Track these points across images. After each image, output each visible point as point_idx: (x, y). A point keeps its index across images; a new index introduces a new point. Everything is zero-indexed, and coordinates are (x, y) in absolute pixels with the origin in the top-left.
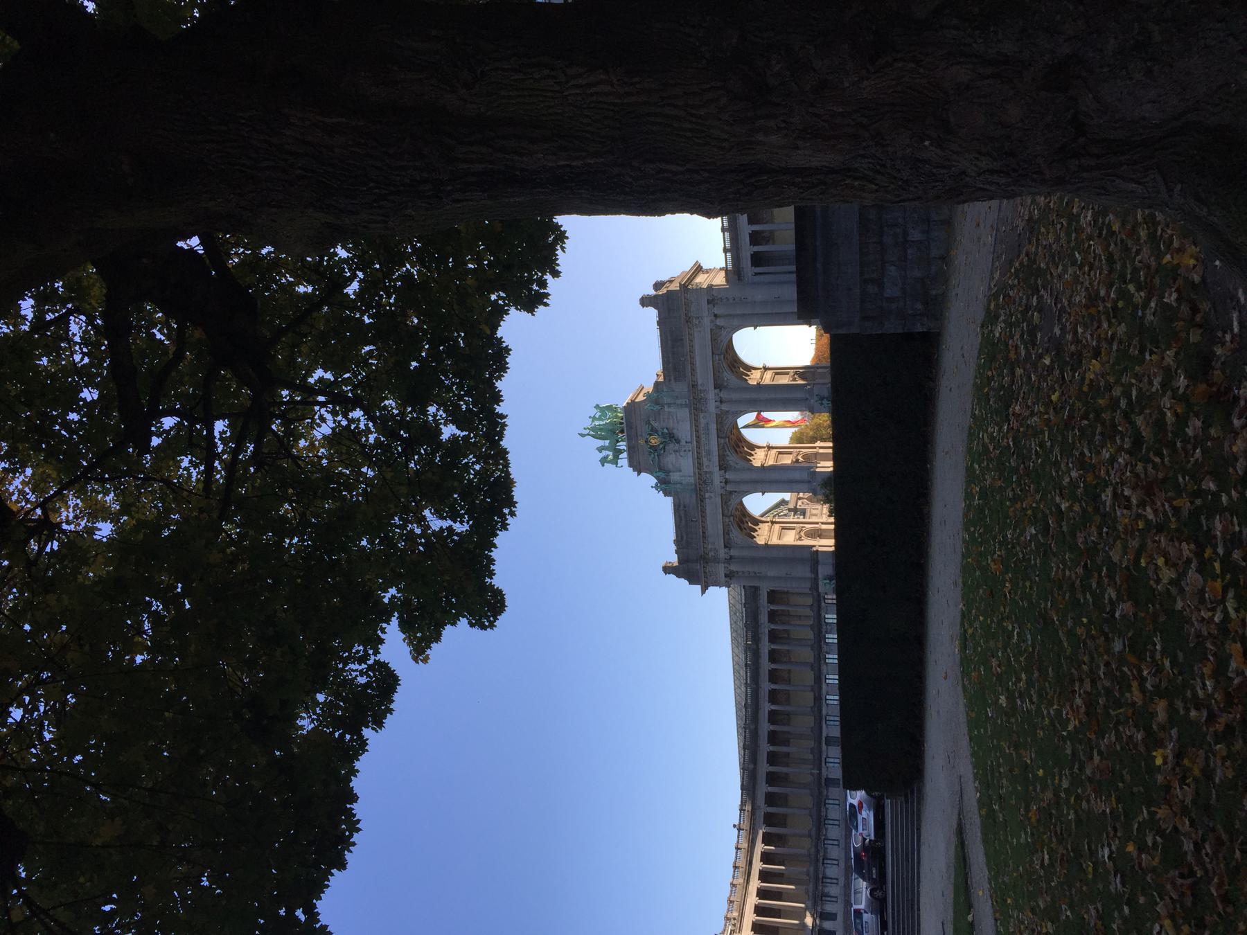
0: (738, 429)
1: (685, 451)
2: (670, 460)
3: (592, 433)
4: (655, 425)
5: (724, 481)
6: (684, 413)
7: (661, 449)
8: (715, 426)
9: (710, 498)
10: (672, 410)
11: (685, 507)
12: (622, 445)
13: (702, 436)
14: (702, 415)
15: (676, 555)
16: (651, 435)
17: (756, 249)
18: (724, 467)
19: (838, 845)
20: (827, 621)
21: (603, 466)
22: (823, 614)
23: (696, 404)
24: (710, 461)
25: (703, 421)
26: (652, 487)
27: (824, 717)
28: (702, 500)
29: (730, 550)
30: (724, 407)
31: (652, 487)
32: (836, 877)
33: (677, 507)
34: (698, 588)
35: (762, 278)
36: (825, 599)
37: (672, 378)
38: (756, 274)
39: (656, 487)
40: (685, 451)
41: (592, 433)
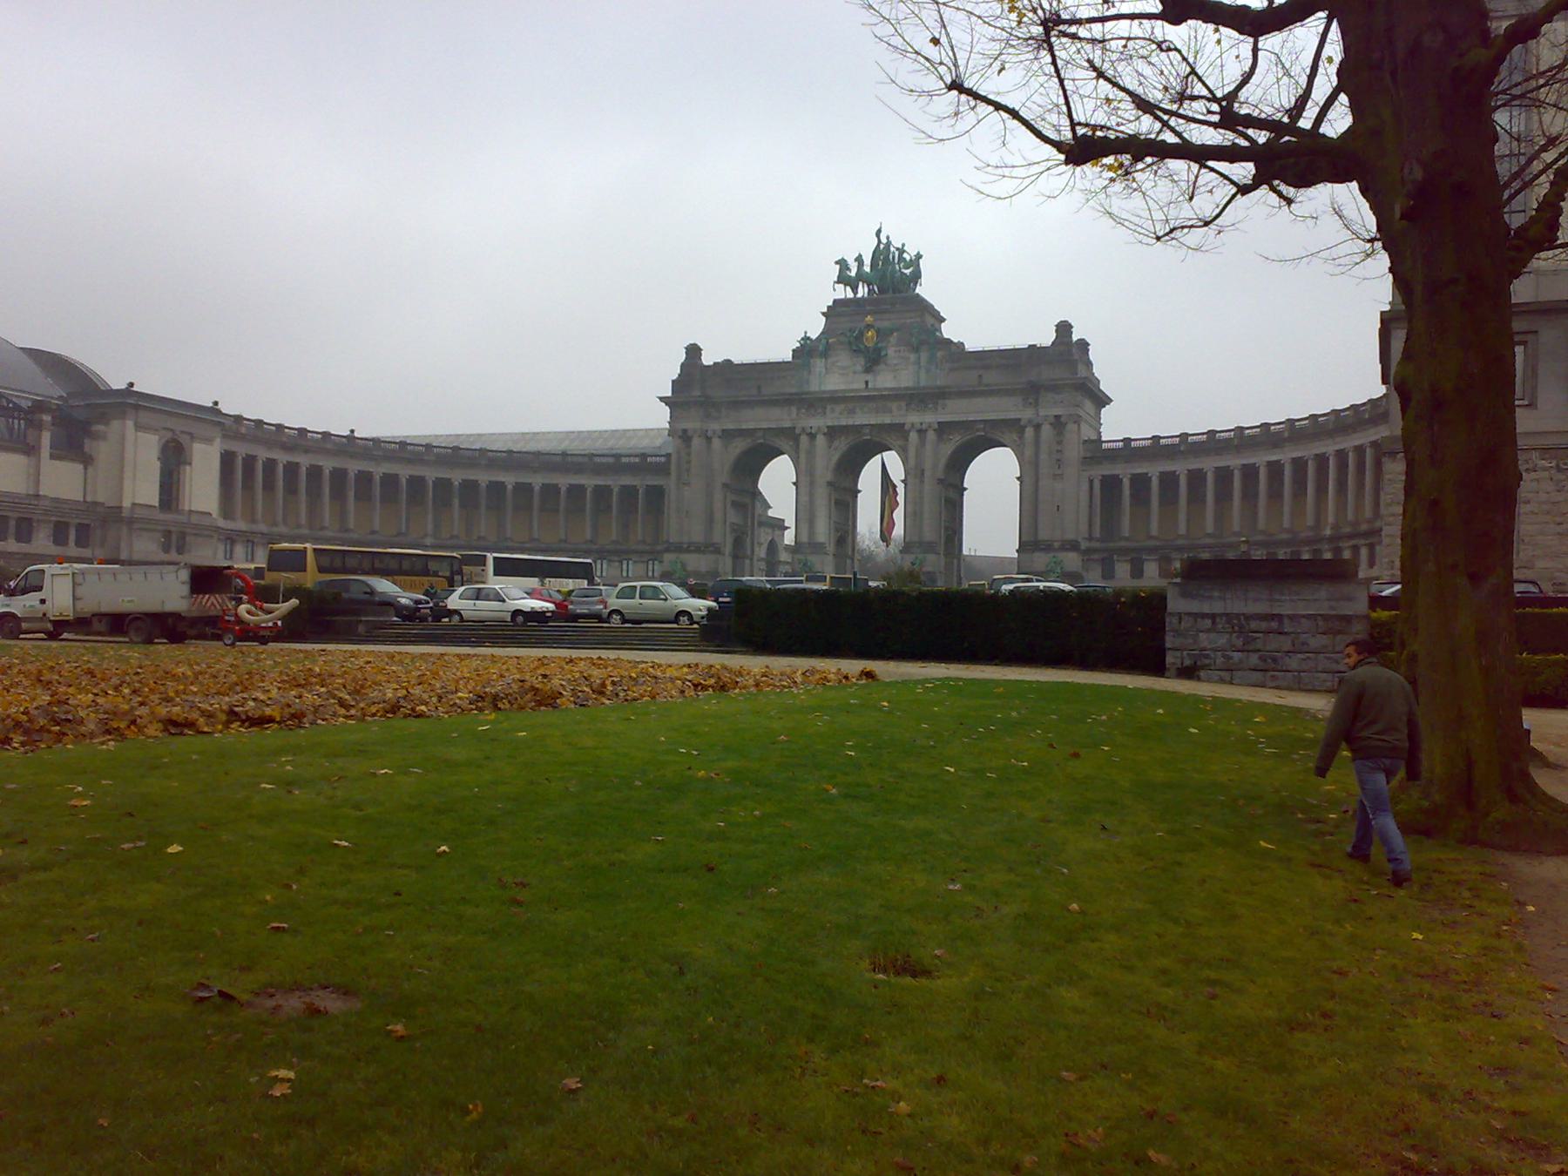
0: (881, 452)
2: (843, 358)
3: (882, 246)
4: (893, 339)
5: (813, 431)
7: (857, 346)
8: (888, 421)
12: (862, 291)
14: (903, 404)
15: (712, 363)
17: (1126, 482)
18: (833, 433)
20: (625, 562)
21: (837, 263)
23: (917, 398)
25: (894, 406)
26: (806, 333)
28: (787, 401)
29: (720, 437)
30: (913, 436)
31: (806, 333)
34: (669, 394)
35: (1085, 486)
36: (653, 560)
38: (1091, 482)
39: (806, 338)
41: (882, 246)
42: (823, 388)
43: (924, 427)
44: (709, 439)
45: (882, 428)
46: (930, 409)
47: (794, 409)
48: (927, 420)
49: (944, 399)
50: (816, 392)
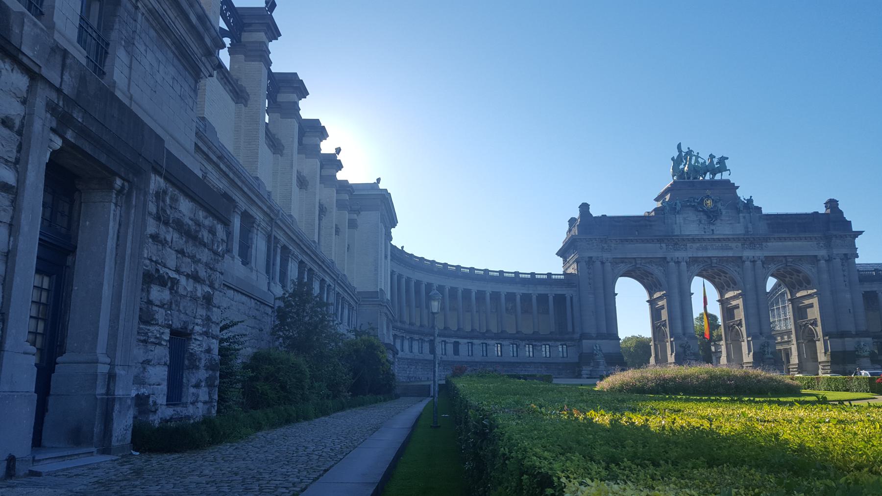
1: (704, 228)
2: (691, 215)
3: (683, 154)
5: (680, 259)
6: (739, 229)
8: (730, 254)
9: (661, 248)
10: (742, 220)
11: (651, 226)
13: (720, 244)
14: (740, 245)
16: (713, 200)
19: (469, 356)
20: (544, 346)
22: (550, 343)
24: (697, 249)
25: (733, 245)
27: (471, 341)
28: (660, 241)
30: (748, 264)
32: (488, 355)
33: (647, 218)
37: (769, 222)
40: (704, 228)
41: (683, 154)
42: (683, 233)
43: (756, 259)
44: (602, 263)
45: (721, 259)
46: (758, 248)
47: (664, 245)
48: (757, 255)
49: (767, 242)
50: (677, 236)
